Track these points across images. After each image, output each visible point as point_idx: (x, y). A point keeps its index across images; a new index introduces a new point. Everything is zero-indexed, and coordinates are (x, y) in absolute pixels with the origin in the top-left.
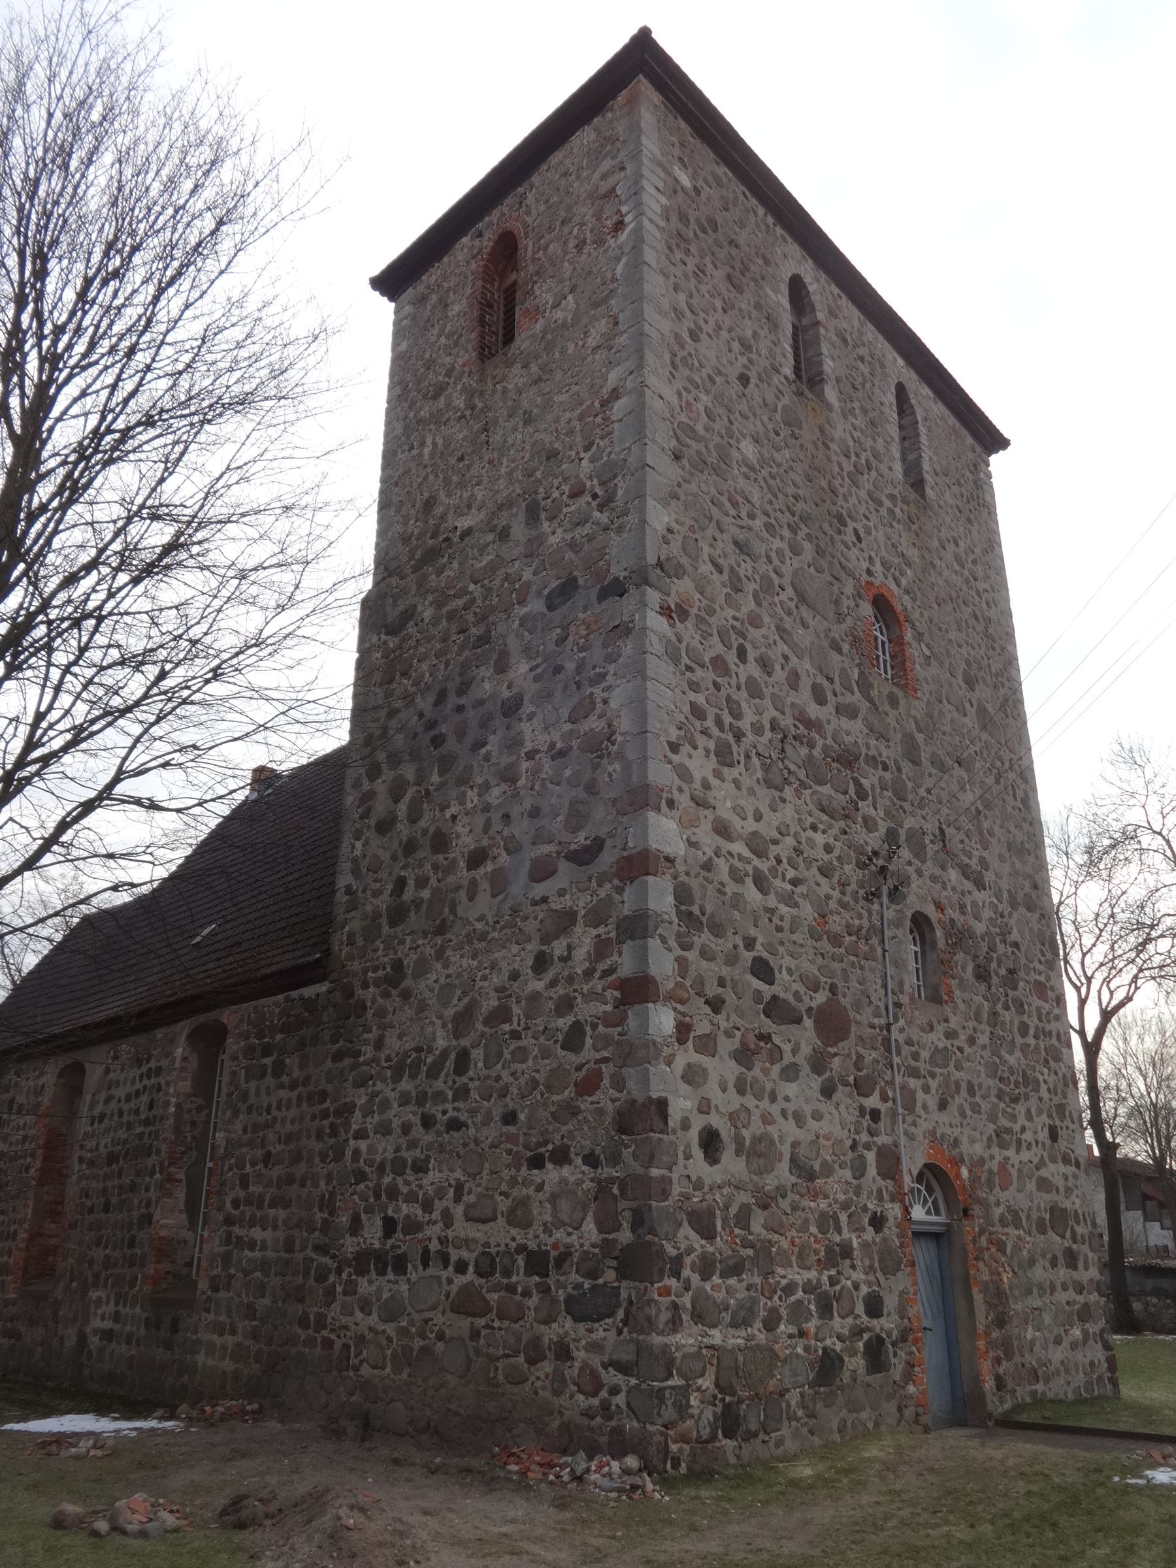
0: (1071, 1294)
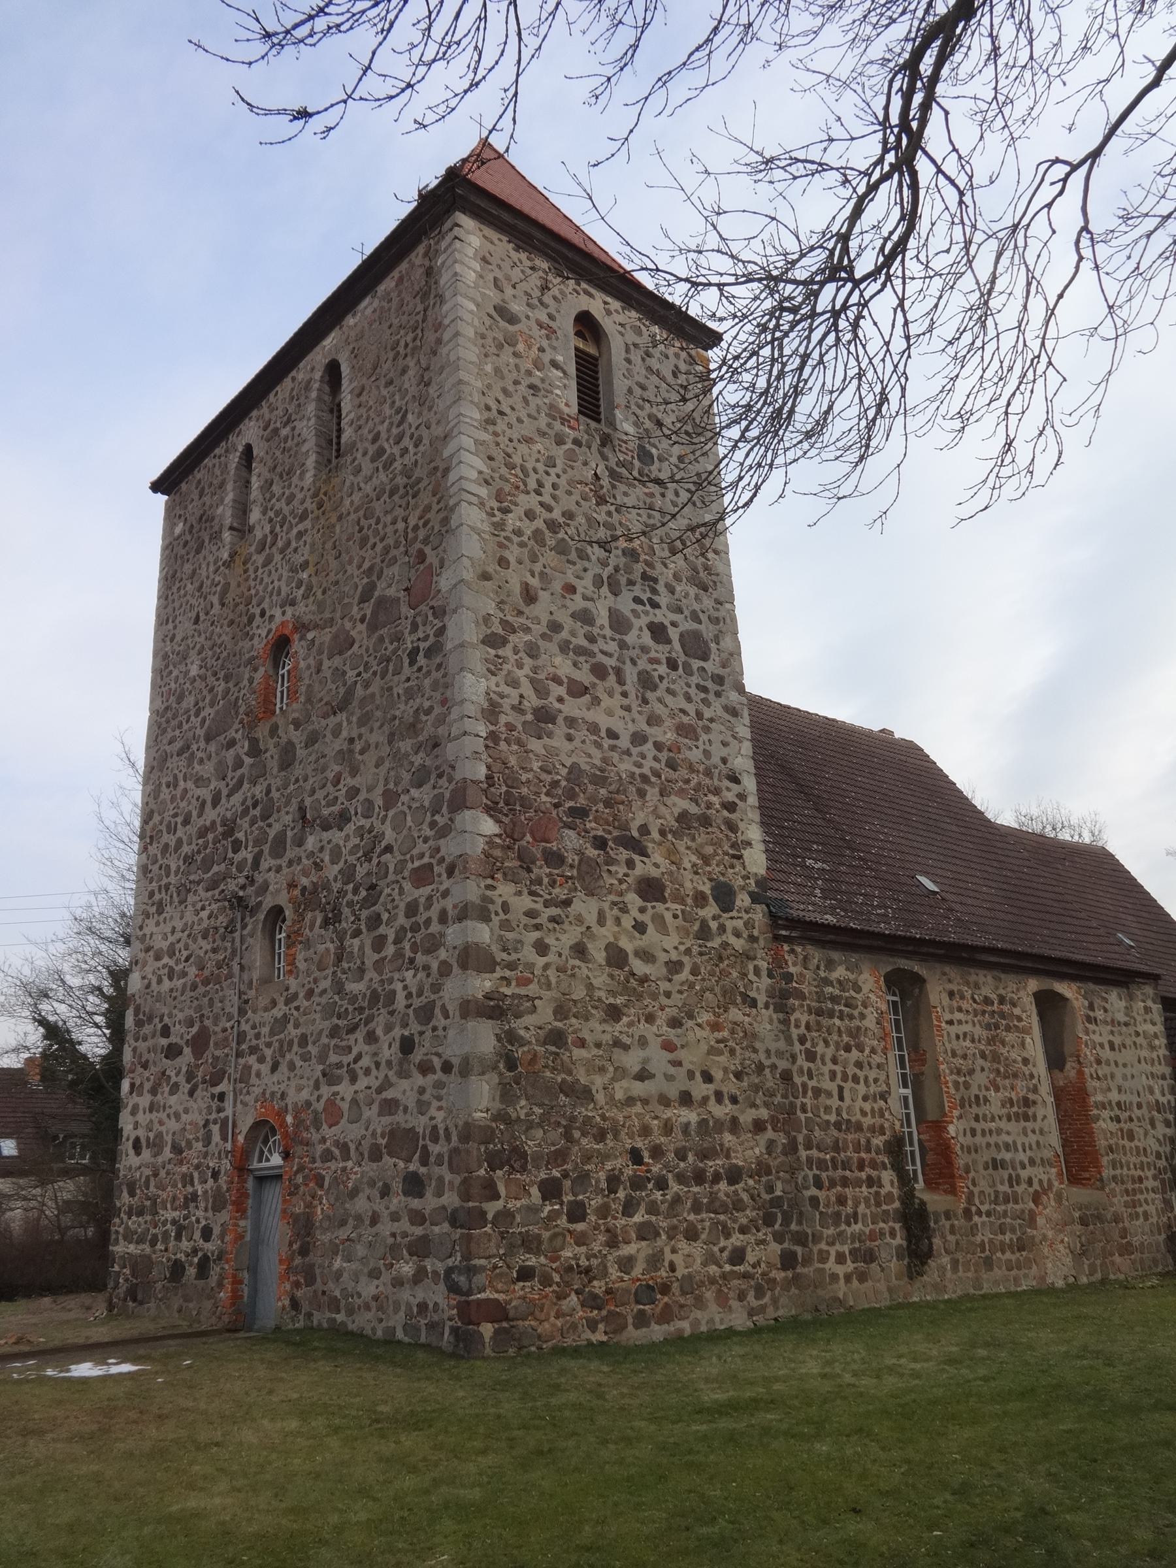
0: (404, 1225)
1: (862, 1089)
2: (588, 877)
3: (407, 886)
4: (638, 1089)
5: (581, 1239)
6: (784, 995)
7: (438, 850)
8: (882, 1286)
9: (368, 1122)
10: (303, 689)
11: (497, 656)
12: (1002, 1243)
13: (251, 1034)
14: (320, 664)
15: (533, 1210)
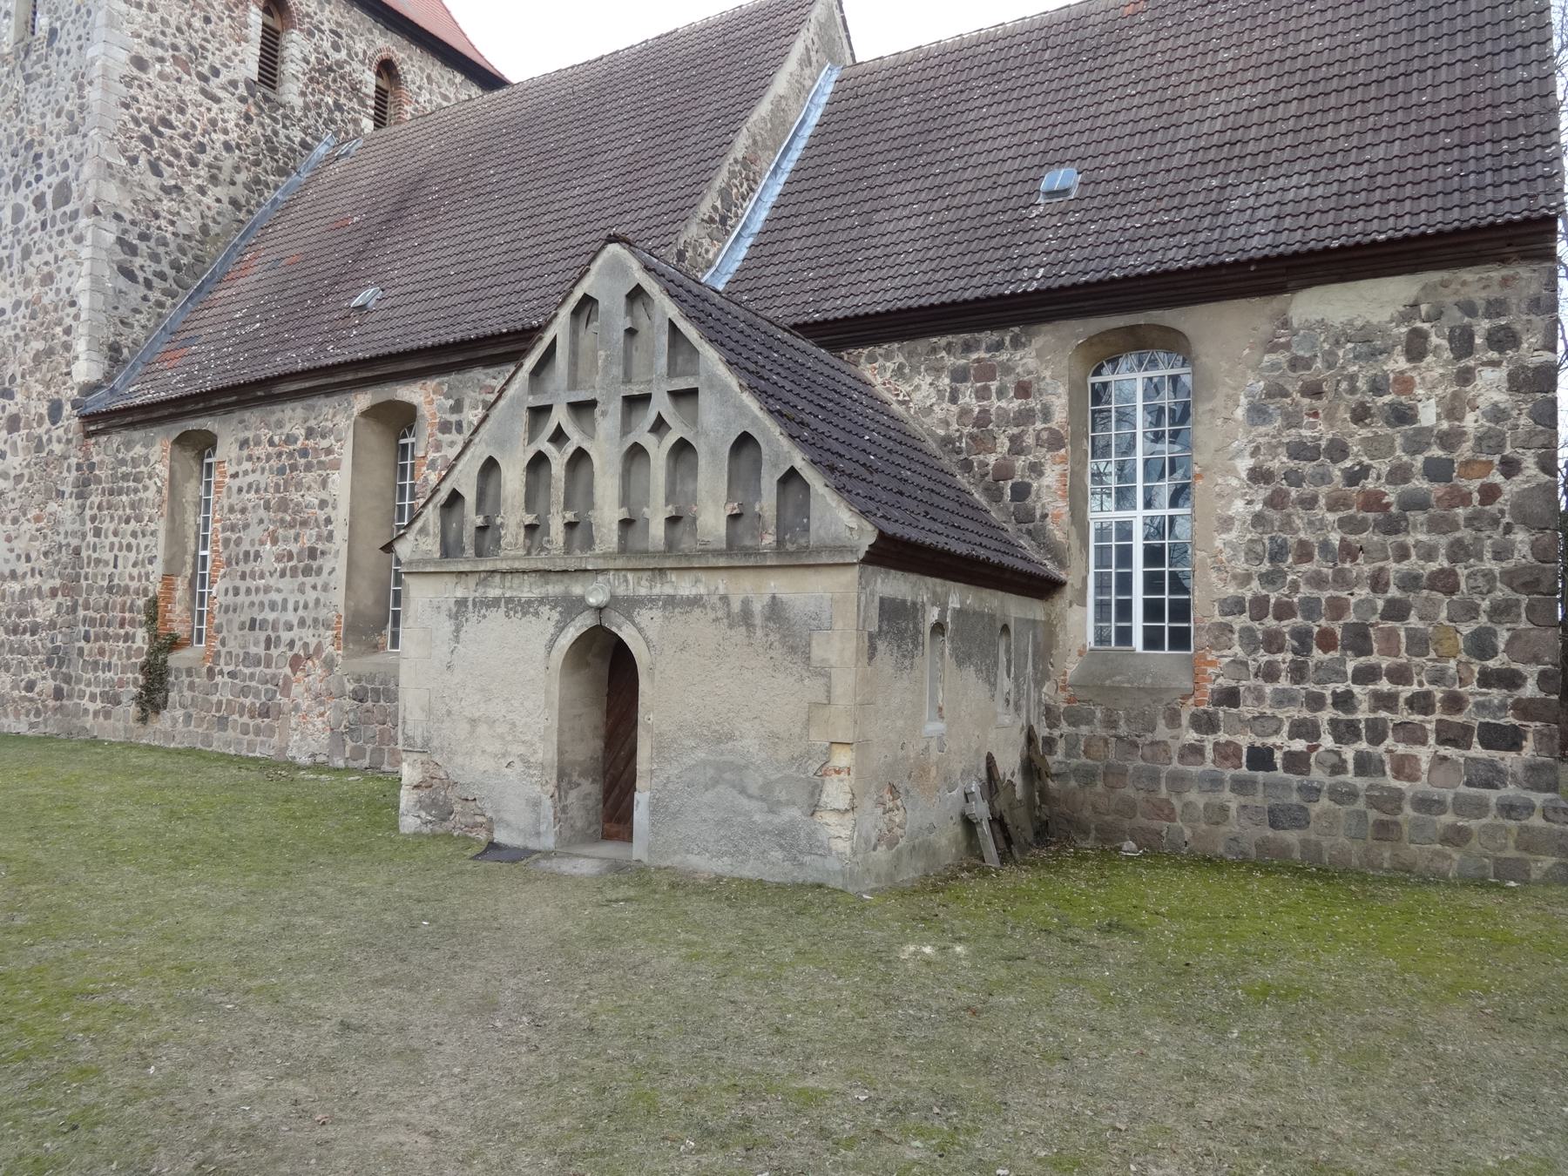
1: (132, 555)
8: (120, 725)
12: (242, 706)
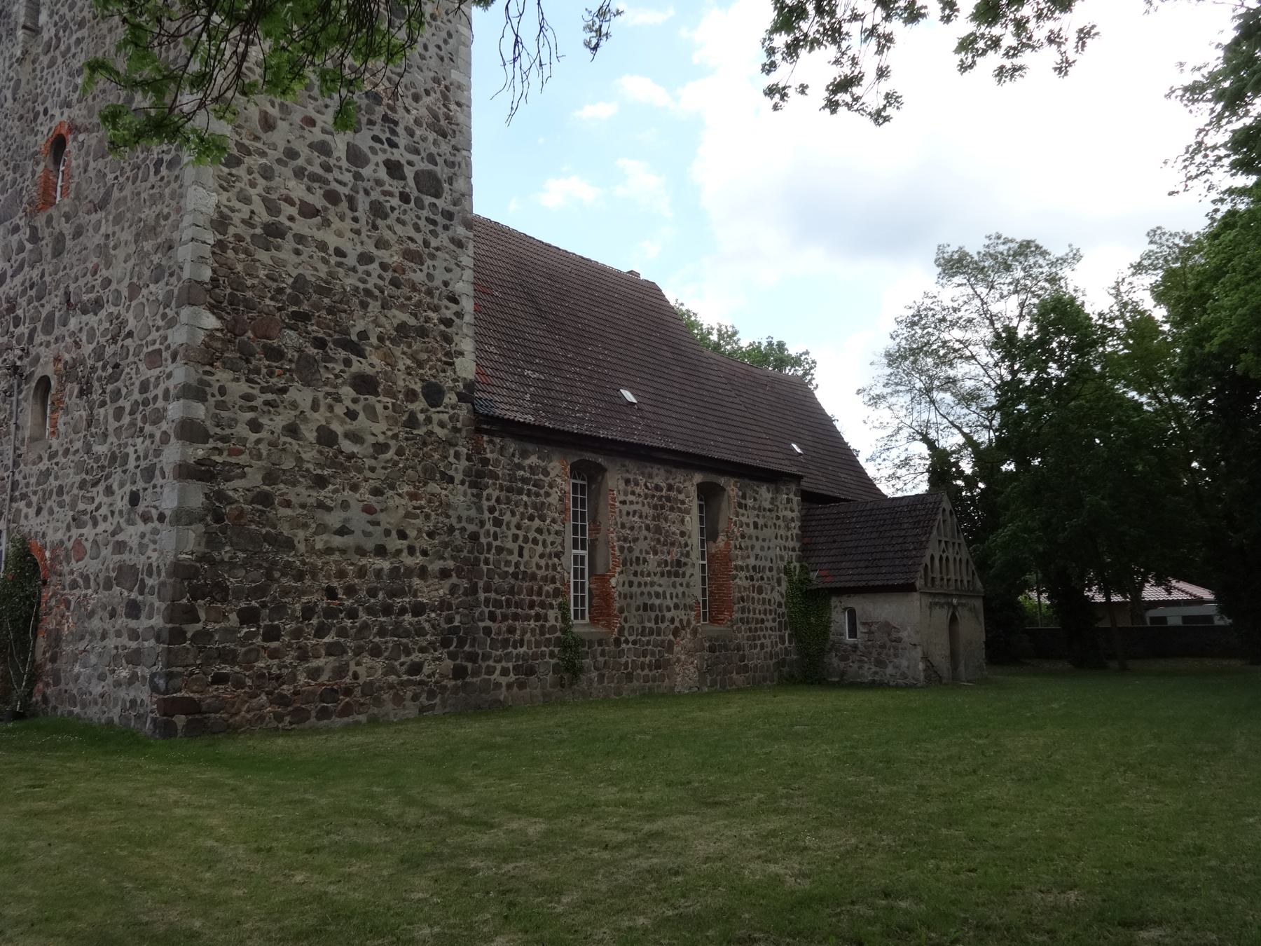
0: (124, 640)
1: (540, 549)
2: (307, 371)
3: (142, 367)
4: (337, 541)
5: (274, 654)
6: (480, 475)
7: (166, 338)
8: (538, 692)
9: (105, 558)
10: (73, 186)
11: (230, 174)
13: (22, 483)
14: (87, 164)
15: (231, 631)
